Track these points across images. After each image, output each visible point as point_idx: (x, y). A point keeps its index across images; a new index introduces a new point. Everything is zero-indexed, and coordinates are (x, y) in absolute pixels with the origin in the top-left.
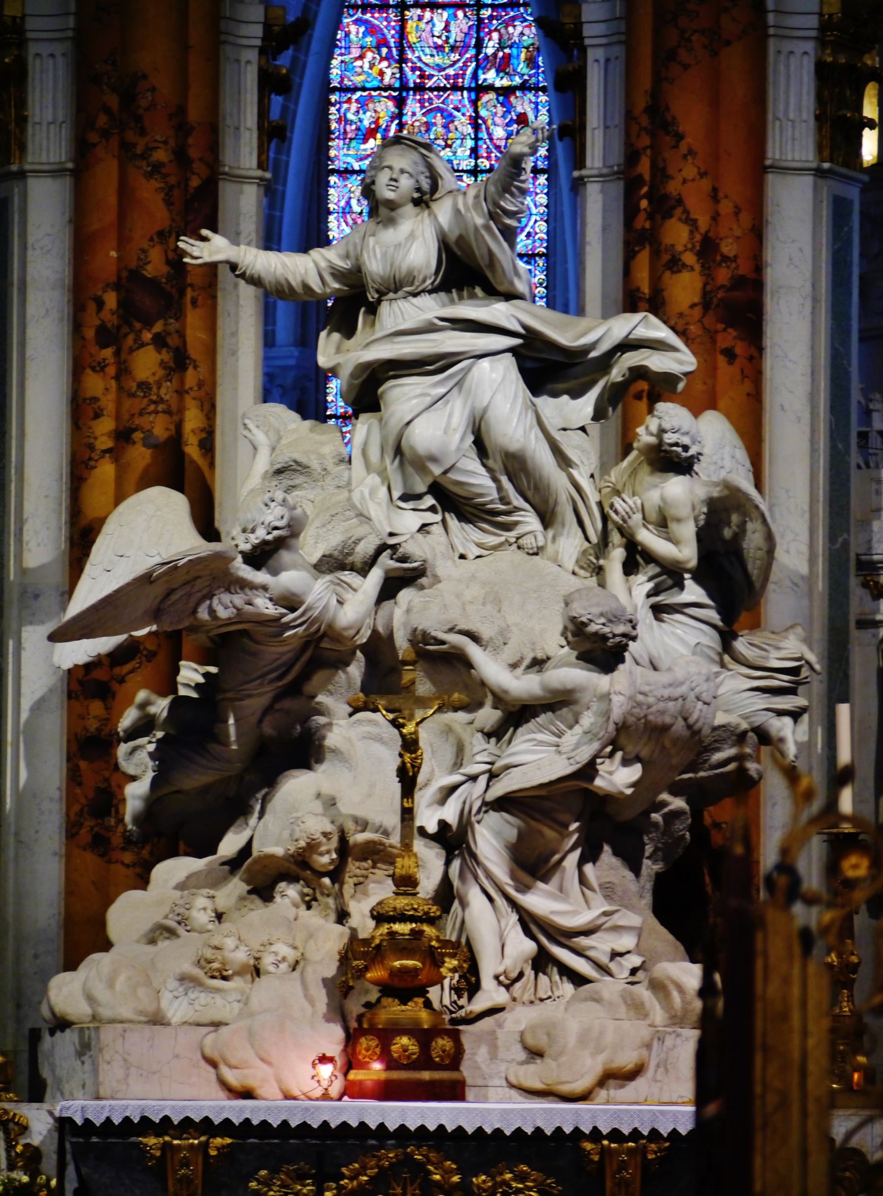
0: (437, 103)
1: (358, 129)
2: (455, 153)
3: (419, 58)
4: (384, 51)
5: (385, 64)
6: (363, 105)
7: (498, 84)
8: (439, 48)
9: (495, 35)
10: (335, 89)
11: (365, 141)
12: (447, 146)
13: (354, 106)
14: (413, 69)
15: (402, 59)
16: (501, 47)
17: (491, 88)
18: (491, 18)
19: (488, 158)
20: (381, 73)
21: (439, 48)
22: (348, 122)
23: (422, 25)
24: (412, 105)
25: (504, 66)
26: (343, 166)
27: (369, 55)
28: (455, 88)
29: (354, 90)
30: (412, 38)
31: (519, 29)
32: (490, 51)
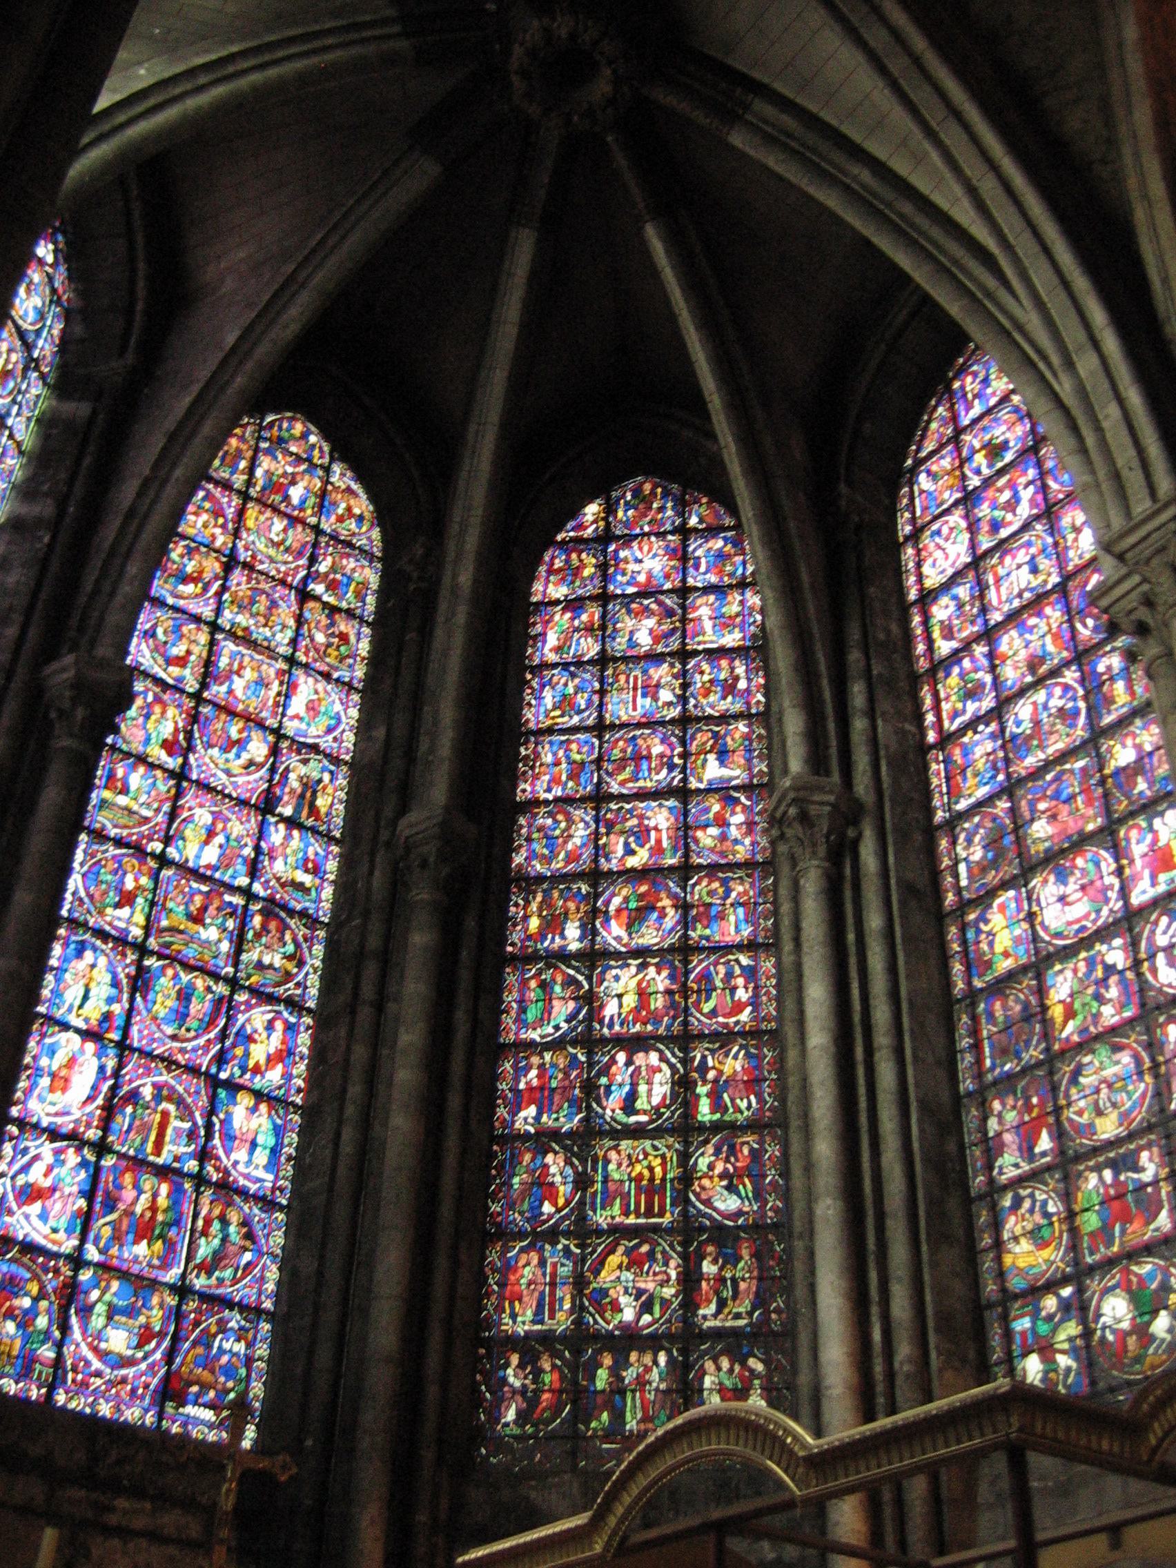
6: (190, 552)
12: (265, 625)
19: (306, 654)
28: (283, 582)
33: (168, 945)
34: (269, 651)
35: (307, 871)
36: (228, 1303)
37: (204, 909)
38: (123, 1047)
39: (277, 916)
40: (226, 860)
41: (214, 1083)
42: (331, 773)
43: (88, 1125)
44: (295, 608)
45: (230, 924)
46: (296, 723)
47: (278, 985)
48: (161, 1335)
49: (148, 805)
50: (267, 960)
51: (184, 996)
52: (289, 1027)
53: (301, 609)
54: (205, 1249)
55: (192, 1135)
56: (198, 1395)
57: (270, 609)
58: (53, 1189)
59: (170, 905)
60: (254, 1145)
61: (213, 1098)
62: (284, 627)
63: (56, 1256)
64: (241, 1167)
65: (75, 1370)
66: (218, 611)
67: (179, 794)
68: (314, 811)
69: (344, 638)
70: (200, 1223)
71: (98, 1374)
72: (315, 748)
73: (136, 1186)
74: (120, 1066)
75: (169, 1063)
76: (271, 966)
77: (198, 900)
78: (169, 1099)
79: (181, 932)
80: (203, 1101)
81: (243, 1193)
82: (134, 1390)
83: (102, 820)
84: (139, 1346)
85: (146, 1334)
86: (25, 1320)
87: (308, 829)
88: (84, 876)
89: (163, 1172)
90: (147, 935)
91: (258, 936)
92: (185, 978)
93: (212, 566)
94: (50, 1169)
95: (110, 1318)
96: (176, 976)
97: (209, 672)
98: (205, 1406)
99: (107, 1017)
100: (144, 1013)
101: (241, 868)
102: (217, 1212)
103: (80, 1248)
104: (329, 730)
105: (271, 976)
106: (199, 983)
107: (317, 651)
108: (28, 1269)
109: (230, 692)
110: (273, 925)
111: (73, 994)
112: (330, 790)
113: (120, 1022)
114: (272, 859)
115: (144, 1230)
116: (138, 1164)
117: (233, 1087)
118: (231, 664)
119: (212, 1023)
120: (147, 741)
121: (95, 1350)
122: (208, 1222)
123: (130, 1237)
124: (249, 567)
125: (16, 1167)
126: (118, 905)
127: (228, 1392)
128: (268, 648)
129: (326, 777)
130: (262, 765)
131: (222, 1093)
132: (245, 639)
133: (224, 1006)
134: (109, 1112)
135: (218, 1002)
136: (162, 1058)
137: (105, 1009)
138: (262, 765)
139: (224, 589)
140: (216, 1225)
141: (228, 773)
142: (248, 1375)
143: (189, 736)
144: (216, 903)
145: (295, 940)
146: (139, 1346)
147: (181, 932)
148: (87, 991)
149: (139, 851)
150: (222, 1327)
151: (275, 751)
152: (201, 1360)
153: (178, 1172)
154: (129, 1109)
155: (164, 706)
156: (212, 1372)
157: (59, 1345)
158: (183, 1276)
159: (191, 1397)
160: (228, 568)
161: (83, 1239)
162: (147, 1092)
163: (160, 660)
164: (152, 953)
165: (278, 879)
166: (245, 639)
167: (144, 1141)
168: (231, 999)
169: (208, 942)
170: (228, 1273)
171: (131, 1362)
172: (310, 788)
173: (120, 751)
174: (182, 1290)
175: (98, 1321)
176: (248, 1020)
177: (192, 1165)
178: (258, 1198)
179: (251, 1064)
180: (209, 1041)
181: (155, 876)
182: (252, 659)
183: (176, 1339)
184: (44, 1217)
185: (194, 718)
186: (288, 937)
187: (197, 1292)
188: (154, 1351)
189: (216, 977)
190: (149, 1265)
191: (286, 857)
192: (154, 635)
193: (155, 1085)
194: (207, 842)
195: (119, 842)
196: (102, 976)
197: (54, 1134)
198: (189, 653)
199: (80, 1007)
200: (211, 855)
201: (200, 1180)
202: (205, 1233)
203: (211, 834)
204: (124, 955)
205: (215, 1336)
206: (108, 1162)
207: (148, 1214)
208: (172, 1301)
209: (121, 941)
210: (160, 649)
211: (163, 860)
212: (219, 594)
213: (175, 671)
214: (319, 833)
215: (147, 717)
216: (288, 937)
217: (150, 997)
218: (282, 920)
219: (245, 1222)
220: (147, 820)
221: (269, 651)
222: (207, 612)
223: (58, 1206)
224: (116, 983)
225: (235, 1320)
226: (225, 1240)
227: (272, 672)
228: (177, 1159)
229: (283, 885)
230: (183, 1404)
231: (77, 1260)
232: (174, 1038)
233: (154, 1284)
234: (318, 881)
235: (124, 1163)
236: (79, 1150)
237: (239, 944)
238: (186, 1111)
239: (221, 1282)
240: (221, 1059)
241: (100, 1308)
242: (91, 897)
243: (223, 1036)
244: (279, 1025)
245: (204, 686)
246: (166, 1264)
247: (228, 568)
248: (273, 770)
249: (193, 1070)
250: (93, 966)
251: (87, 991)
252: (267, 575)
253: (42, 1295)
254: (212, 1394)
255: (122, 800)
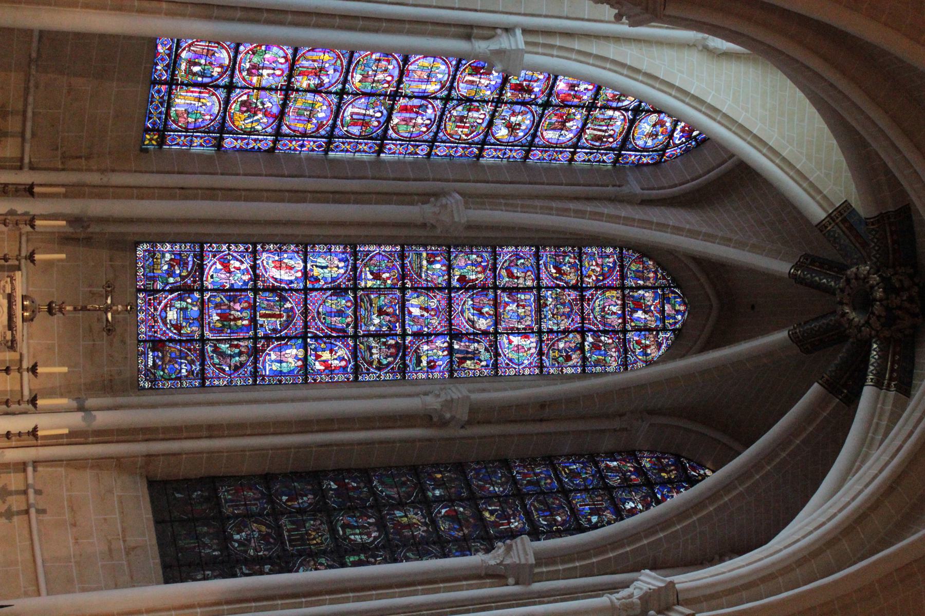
0: (575, 308)
1: (561, 263)
2: (550, 320)
3: (597, 298)
4: (601, 278)
5: (594, 278)
6: (572, 266)
7: (586, 343)
8: (603, 309)
9: (610, 341)
10: (580, 249)
11: (555, 267)
13: (572, 261)
14: (592, 295)
15: (597, 288)
16: (605, 344)
17: (584, 340)
18: (619, 338)
19: (548, 339)
20: (589, 276)
21: (603, 309)
22: (564, 257)
23: (614, 299)
24: (574, 294)
25: (595, 346)
26: (541, 254)
27: (598, 269)
28: (583, 319)
29: (581, 261)
30: (608, 294)
31: (614, 355)
32: (603, 338)
33: (362, 300)
34: (539, 321)
35: (428, 363)
36: (203, 364)
37: (388, 314)
38: (306, 291)
39: (398, 351)
40: (415, 319)
41: (304, 337)
42: (487, 366)
43: (264, 282)
44: (571, 328)
45: (385, 329)
46: (506, 341)
47: (364, 359)
48: (180, 334)
49: (427, 276)
50: (374, 351)
51: (340, 313)
52: (345, 368)
53: (572, 331)
54: (224, 347)
55: (274, 330)
56: (158, 357)
57: (563, 314)
58: (230, 272)
59: (382, 298)
60: (281, 362)
61: (296, 337)
62: (558, 324)
63: (202, 281)
64: (268, 357)
65: (154, 299)
66: (548, 288)
67: (441, 289)
68: (462, 360)
69: (568, 358)
70: (236, 343)
71: (156, 309)
72: (497, 355)
73: (243, 309)
74: (297, 290)
75: (306, 312)
76: (372, 354)
77: (390, 310)
78: (288, 316)
79: (371, 305)
80: (293, 333)
81: (256, 361)
82: (153, 327)
83: (411, 256)
84: (172, 325)
85: (178, 327)
86: (170, 273)
87: (451, 358)
88: (379, 254)
89: (253, 320)
90: (363, 289)
91: (384, 344)
92: (350, 312)
93: (572, 279)
94: (239, 269)
95: (181, 309)
96: (349, 307)
97: (512, 291)
98: (154, 361)
99: (317, 280)
100: (325, 296)
101: (415, 329)
102: (243, 350)
103: (207, 290)
104: (511, 360)
105: (367, 354)
106: (349, 319)
107: (553, 345)
108: (192, 269)
109: (507, 304)
110: (392, 350)
111: (321, 261)
112: (477, 367)
113: (317, 286)
114: (427, 343)
115: (224, 317)
116: (253, 308)
117: (305, 346)
118: (522, 300)
119: (333, 330)
120: (460, 268)
121: (166, 306)
122: (237, 346)
123: (219, 311)
124: (582, 298)
125: (235, 254)
126: (372, 273)
127: (163, 370)
128: (541, 318)
129: (484, 363)
130: (474, 328)
131: (300, 341)
132: (540, 306)
133: (342, 335)
134: (273, 290)
135: (343, 330)
136: (306, 309)
137: (320, 277)
138: (474, 328)
139: (563, 288)
140: (237, 351)
141: (462, 312)
142: (172, 379)
143: (473, 287)
144: (393, 319)
145: (389, 364)
146: (172, 325)
147: (371, 305)
148: (326, 267)
149: (403, 277)
150: (192, 362)
151: (485, 333)
152: (173, 355)
153: (255, 329)
154: (277, 299)
155: (484, 271)
156: (170, 361)
157: (163, 290)
158: (209, 340)
159: (156, 354)
160: (574, 287)
161: (211, 290)
162: (288, 305)
163: (506, 264)
164: (355, 294)
165: (418, 348)
166: (540, 306)
167: (265, 309)
168: (348, 337)
169: (371, 320)
170: (217, 361)
171: (165, 324)
172: (475, 356)
173: (450, 256)
174: (203, 340)
175: (178, 304)
176: (340, 347)
177: (261, 334)
178: (255, 368)
179: (320, 353)
180: (323, 330)
181: (392, 288)
182: (531, 311)
183: (180, 341)
184: (216, 271)
185: (484, 288)
186: (390, 359)
187: (203, 348)
188: (172, 332)
189: (356, 327)
190: (209, 323)
191: (432, 350)
192: (518, 259)
193: (292, 308)
194: (421, 308)
195: (403, 266)
196: (335, 272)
197: (254, 267)
198: (518, 278)
199: (317, 266)
200: (416, 312)
201: (255, 338)
202: (231, 346)
203: (426, 309)
204: (349, 280)
205: (186, 359)
206: (251, 295)
207: (232, 317)
208: (196, 337)
209: (356, 278)
210: (512, 263)
211: (403, 289)
212: (558, 286)
213: (504, 273)
214: (451, 366)
215: (472, 265)
216: (390, 359)
217: (334, 298)
218: (397, 355)
219: (242, 365)
220: (420, 277)
221: (539, 321)
222: (545, 282)
223: (223, 276)
224: (334, 280)
225: (197, 368)
226: (231, 356)
227: (529, 323)
228: (262, 326)
229: (415, 351)
230: (153, 351)
231: (202, 290)
232: (318, 313)
233: (202, 327)
234: (425, 369)
235: (252, 301)
236: (250, 279)
237: (377, 335)
238: (285, 326)
239: (211, 358)
240: (316, 337)
241: (184, 304)
242: (371, 259)
243: (329, 337)
244: (343, 363)
245: (504, 289)
246: (211, 330)
247: (574, 287)
248: (475, 334)
249: (306, 326)
250: (338, 267)
251: (326, 267)
252: (582, 309)
253: (183, 278)
254: (160, 363)
255: (425, 263)
